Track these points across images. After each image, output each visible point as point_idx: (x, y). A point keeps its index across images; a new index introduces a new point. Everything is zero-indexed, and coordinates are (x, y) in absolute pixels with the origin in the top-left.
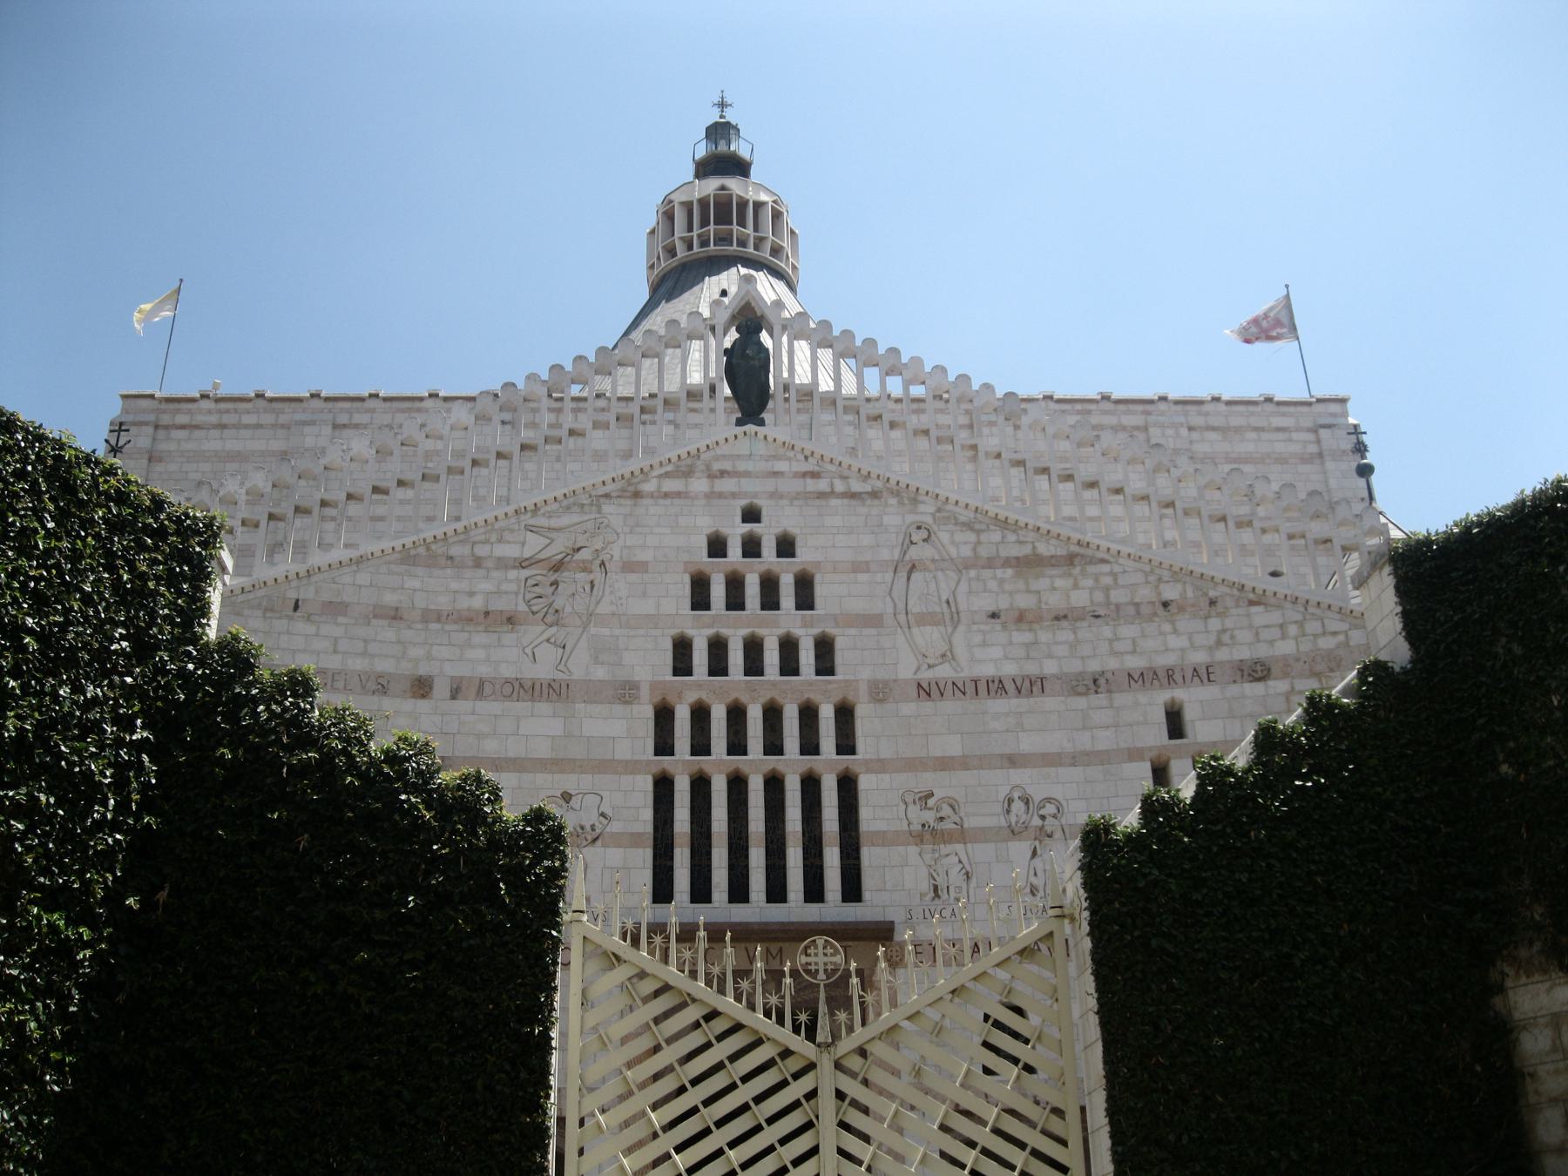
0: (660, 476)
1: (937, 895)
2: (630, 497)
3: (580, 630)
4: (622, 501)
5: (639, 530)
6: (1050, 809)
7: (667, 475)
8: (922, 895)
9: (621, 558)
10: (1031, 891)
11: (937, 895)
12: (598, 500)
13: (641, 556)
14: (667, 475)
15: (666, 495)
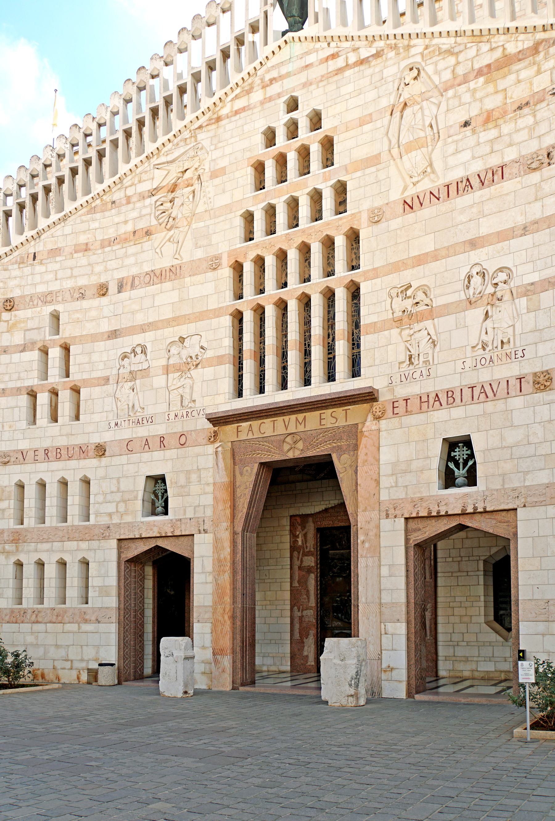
0: (232, 100)
1: (411, 363)
2: (214, 123)
3: (188, 227)
4: (210, 128)
5: (220, 145)
6: (502, 276)
7: (237, 97)
8: (400, 363)
9: (210, 169)
10: (483, 347)
11: (411, 363)
12: (195, 133)
13: (221, 164)
14: (237, 97)
15: (237, 113)
